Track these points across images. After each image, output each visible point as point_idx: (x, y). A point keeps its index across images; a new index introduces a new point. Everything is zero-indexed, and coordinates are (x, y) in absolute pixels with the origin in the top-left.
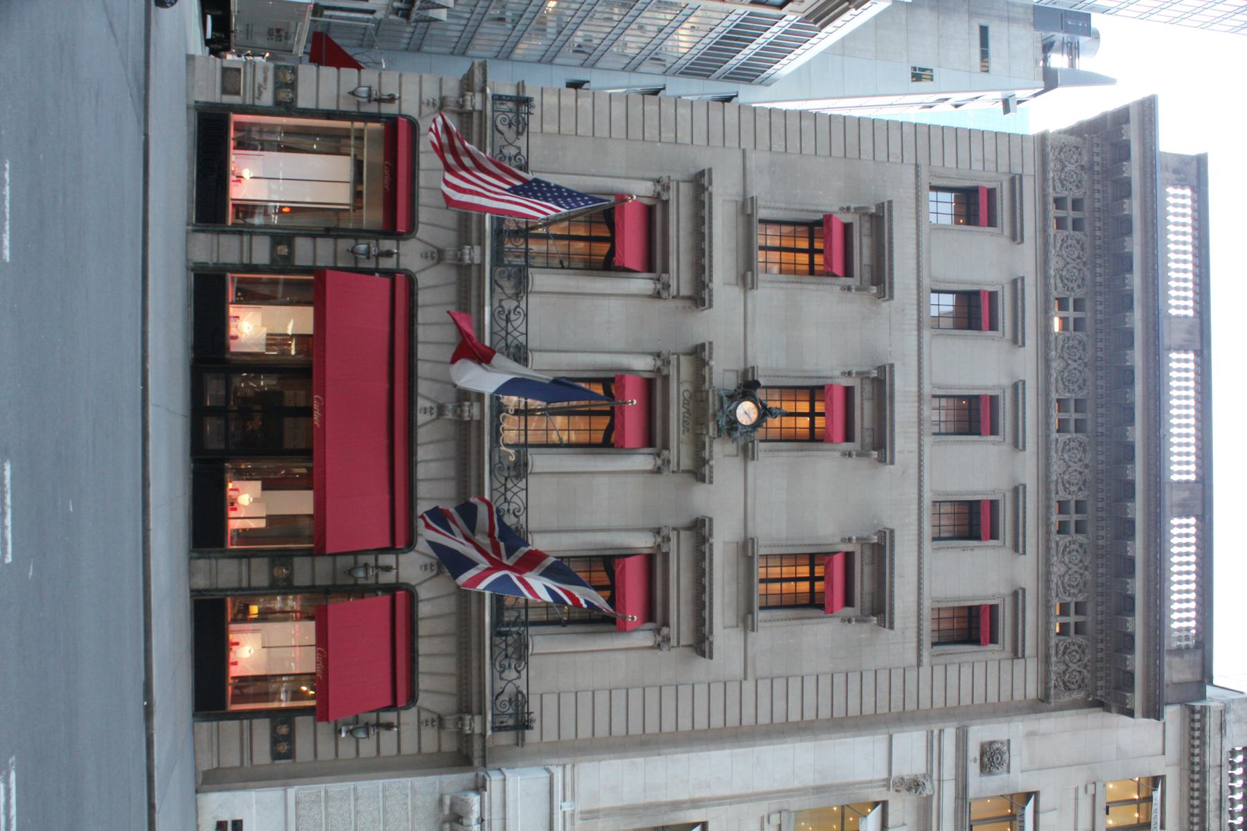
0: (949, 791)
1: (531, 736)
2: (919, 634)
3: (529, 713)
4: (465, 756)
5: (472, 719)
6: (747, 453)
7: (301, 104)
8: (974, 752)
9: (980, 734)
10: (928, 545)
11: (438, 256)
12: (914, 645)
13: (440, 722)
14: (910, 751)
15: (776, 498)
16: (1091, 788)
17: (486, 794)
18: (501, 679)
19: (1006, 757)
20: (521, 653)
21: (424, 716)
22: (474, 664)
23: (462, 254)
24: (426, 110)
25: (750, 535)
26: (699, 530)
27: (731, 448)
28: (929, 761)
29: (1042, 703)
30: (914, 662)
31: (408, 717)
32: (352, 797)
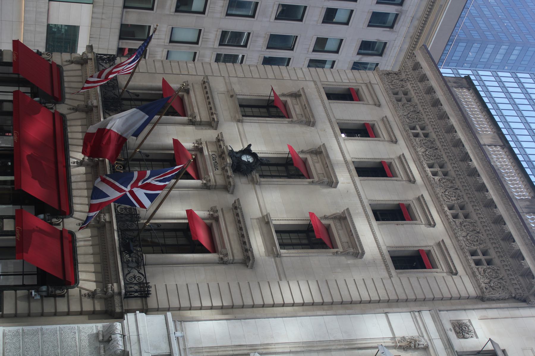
0: (439, 344)
1: (152, 302)
3: (147, 283)
4: (113, 314)
5: (113, 285)
6: (254, 182)
7: (5, 60)
8: (448, 326)
9: (448, 317)
11: (76, 109)
12: (383, 267)
13: (92, 295)
15: (277, 203)
17: (125, 321)
18: (128, 267)
19: (471, 328)
20: (140, 264)
21: (83, 292)
22: (111, 262)
23: (107, 289)
24: (66, 63)
25: (265, 214)
26: (237, 209)
27: (244, 180)
29: (482, 299)
30: (386, 275)
31: (74, 292)
32: (40, 333)
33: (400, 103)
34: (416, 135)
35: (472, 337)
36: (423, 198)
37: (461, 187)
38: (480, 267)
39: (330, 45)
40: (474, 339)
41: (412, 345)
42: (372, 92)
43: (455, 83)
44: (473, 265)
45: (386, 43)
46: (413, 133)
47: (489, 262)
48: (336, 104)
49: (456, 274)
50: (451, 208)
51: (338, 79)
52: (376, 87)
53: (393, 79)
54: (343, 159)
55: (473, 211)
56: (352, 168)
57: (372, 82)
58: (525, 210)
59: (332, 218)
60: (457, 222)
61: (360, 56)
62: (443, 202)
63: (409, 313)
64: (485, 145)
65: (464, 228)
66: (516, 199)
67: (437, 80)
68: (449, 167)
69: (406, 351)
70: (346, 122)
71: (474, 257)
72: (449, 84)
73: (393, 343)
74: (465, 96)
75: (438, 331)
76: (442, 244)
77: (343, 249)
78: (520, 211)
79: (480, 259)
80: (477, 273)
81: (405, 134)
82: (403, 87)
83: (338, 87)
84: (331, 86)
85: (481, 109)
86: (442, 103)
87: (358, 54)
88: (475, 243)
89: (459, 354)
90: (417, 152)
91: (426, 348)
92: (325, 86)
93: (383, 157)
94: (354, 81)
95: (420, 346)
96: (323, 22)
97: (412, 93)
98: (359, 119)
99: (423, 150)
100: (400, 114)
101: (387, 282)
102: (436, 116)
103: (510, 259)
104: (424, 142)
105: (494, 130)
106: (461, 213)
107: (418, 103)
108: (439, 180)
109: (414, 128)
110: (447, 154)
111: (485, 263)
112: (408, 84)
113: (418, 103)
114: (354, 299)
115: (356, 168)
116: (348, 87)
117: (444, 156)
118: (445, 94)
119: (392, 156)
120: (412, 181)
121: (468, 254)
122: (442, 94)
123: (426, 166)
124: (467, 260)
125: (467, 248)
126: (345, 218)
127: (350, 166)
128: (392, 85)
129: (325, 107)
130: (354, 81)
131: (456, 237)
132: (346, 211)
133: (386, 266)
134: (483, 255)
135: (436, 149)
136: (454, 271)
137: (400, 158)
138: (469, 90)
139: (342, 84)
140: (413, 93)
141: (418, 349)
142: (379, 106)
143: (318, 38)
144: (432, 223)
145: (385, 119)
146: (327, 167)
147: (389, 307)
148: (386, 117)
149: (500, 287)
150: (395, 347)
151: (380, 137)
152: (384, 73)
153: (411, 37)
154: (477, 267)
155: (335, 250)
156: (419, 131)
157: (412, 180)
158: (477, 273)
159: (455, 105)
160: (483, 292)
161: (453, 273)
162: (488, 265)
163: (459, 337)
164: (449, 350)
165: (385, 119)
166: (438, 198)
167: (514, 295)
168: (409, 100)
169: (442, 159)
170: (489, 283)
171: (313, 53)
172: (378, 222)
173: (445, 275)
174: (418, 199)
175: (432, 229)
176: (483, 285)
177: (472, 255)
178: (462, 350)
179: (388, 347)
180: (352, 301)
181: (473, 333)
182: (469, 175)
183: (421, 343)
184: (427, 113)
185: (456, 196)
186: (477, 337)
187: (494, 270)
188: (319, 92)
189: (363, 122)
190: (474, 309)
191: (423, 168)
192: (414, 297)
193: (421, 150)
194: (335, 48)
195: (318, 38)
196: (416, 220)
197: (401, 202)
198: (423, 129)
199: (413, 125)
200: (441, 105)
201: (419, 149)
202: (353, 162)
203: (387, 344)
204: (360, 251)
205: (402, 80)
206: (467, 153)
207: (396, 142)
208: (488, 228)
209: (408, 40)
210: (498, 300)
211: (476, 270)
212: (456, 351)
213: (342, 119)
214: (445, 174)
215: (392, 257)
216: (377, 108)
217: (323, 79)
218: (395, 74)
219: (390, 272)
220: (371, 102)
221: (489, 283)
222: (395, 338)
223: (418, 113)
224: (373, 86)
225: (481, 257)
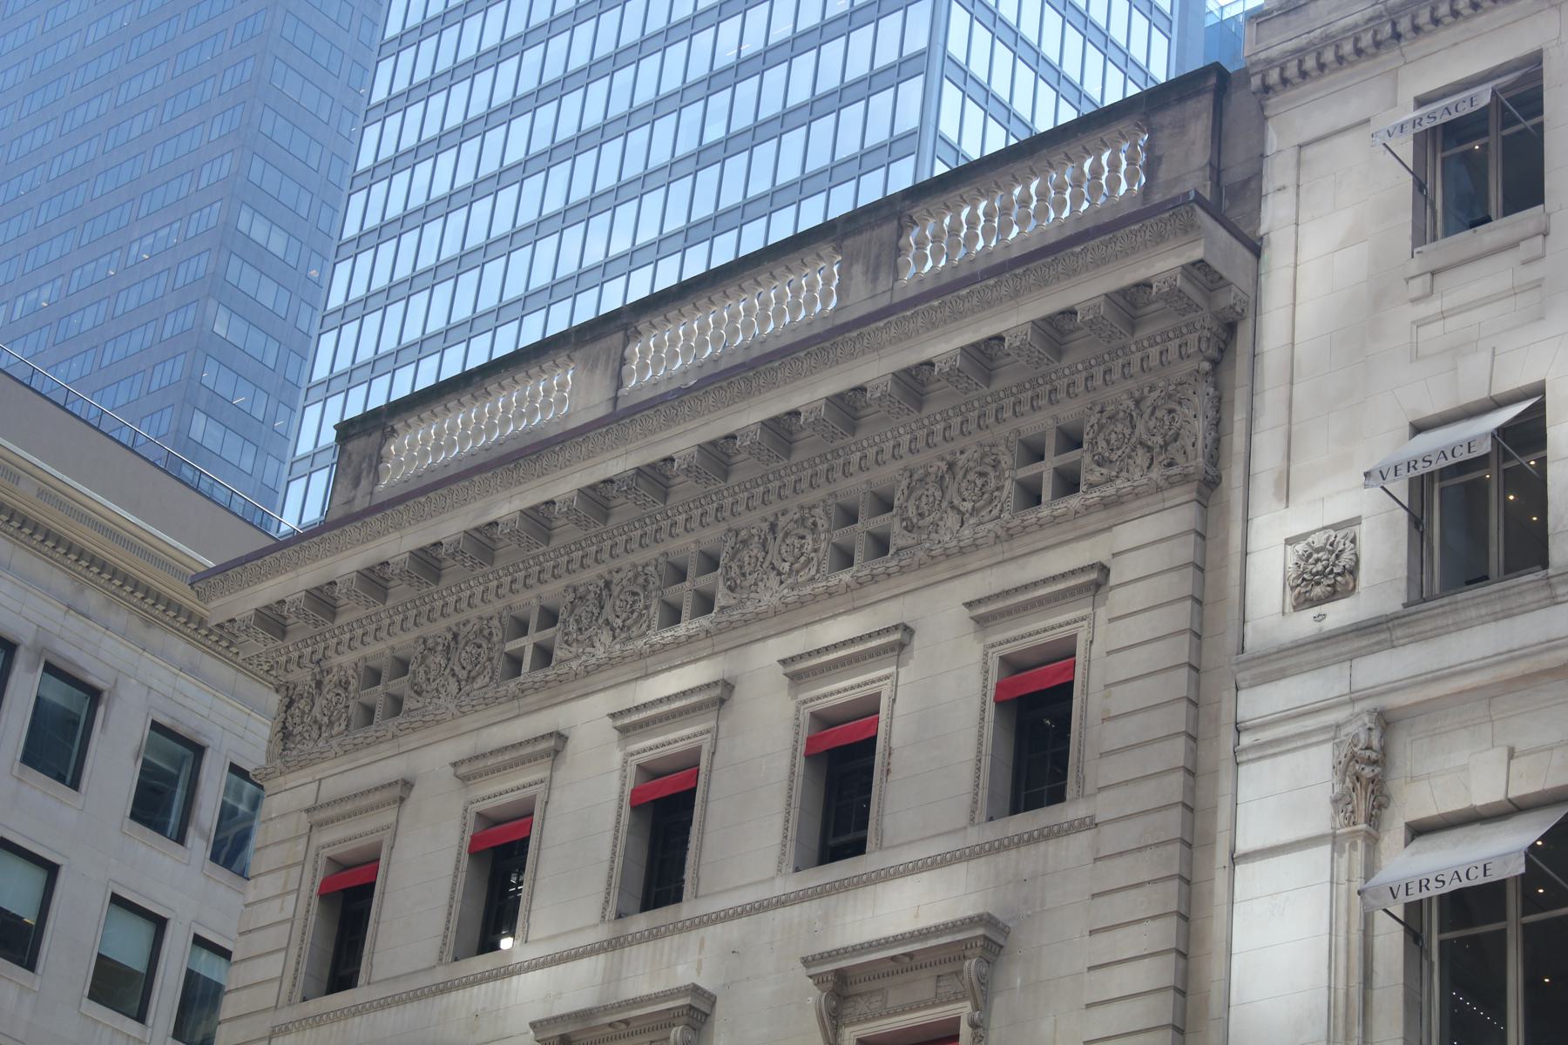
2: (1031, 839)
10: (869, 862)
12: (1050, 847)
14: (1280, 798)
16: (1417, 287)
19: (1319, 540)
28: (1302, 741)
29: (1209, 485)
33: (407, 705)
34: (544, 655)
35: (1353, 541)
36: (792, 659)
37: (769, 511)
38: (1085, 477)
39: (131, 954)
40: (1363, 531)
41: (1368, 772)
42: (349, 807)
43: (356, 483)
44: (1074, 502)
45: (156, 726)
46: (533, 668)
47: (1071, 440)
48: (377, 958)
49: (1104, 570)
50: (845, 558)
51: (278, 937)
52: (336, 786)
53: (307, 720)
54: (602, 957)
55: (864, 476)
56: (641, 922)
57: (310, 803)
58: (884, 283)
59: (836, 1029)
60: (901, 543)
61: (192, 834)
62: (820, 586)
63: (1242, 769)
64: (616, 399)
65: (929, 519)
66: (837, 310)
67: (338, 550)
68: (684, 546)
69: (1388, 798)
70: (453, 926)
71: (1046, 494)
72: (360, 504)
73: (1353, 846)
74: (414, 451)
75: (1320, 665)
76: (982, 610)
77: (964, 998)
78: (883, 302)
79: (1055, 474)
80: (1109, 491)
81: (532, 699)
82: (345, 685)
83: (308, 938)
84: (303, 968)
85: (475, 398)
86: (433, 540)
87: (180, 839)
88: (993, 484)
89: (1416, 596)
90: (611, 663)
91: (1385, 722)
92: (298, 994)
93: (615, 796)
94: (296, 871)
95: (1375, 743)
96: (31, 965)
97: (377, 650)
98: (451, 870)
99: (606, 636)
100: (452, 707)
101: (1112, 838)
102: (478, 571)
103: (1067, 361)
104: (573, 627)
105: (561, 359)
106: (870, 523)
107: (415, 633)
108: (731, 589)
109: (515, 662)
110: (634, 545)
111: (1073, 456)
112: (336, 660)
113: (415, 633)
114: (1168, 979)
115: (645, 907)
116: (315, 901)
117: (639, 557)
118: (398, 527)
119: (617, 757)
120: (721, 696)
121: (1031, 516)
122: (396, 535)
123: (668, 635)
124: (1055, 520)
125: (1006, 516)
126: (841, 975)
127: (633, 929)
128: (331, 724)
129: (383, 1004)
130: (296, 871)
131: (962, 551)
132: (814, 971)
133: (1047, 834)
134: (1041, 457)
135: (608, 584)
136: (1093, 576)
137: (624, 731)
138: (393, 431)
139: (298, 924)
140: (373, 649)
141: (1384, 750)
142: (407, 785)
143: (92, 996)
144: (896, 636)
145: (463, 770)
146: (626, 1022)
147: (1211, 843)
148: (454, 765)
149: (1170, 411)
150: (1372, 841)
151: (532, 800)
152: (278, 750)
153: (148, 624)
154: (1083, 488)
155: (965, 1031)
156: (527, 644)
157: (716, 692)
158: (1109, 491)
159: (444, 491)
160: (1185, 478)
161: (1097, 581)
162: (1080, 445)
163: (1350, 591)
164: (1399, 633)
165: (463, 770)
166: (801, 603)
167: (1206, 366)
168: (402, 666)
169: (651, 569)
170: (1150, 449)
171: (150, 1021)
172: (870, 846)
173: (1102, 614)
174: (797, 679)
175: (917, 642)
176: (1156, 474)
177: (1037, 500)
178: (1403, 585)
179: (1370, 869)
180: (1176, 989)
181: (1341, 534)
182: (725, 475)
183: (1363, 737)
184: (464, 605)
185: (801, 531)
186: (1356, 521)
187: (1101, 427)
188: (317, 1020)
189: (465, 857)
190: (1247, 521)
191: (677, 643)
192: (1181, 744)
193: (604, 646)
194: (145, 930)
195: (92, 996)
196: (876, 698)
197: (802, 748)
198: (521, 628)
199: (500, 664)
200: (438, 544)
201: (600, 652)
202: (619, 916)
203: (1358, 871)
204: (980, 931)
205: (319, 684)
206: (639, 471)
207: (561, 738)
208: (939, 427)
209: (156, 637)
210: (1218, 425)
211: (1095, 495)
212: (1405, 606)
213: (439, 941)
214: (711, 562)
215: (1015, 810)
216: (415, 794)
217: (268, 996)
218: (289, 707)
219: (1071, 824)
220: (388, 816)
221: (1150, 449)
222: (1334, 836)
223: (455, 636)
224: (325, 796)
225: (1046, 470)
